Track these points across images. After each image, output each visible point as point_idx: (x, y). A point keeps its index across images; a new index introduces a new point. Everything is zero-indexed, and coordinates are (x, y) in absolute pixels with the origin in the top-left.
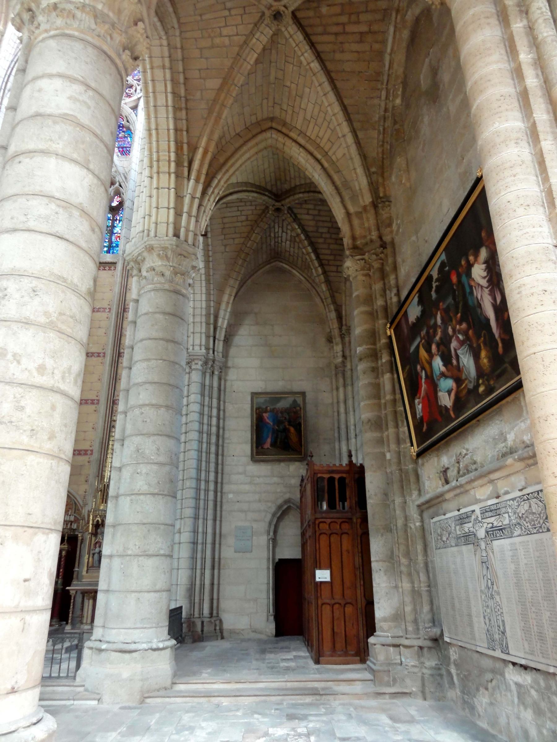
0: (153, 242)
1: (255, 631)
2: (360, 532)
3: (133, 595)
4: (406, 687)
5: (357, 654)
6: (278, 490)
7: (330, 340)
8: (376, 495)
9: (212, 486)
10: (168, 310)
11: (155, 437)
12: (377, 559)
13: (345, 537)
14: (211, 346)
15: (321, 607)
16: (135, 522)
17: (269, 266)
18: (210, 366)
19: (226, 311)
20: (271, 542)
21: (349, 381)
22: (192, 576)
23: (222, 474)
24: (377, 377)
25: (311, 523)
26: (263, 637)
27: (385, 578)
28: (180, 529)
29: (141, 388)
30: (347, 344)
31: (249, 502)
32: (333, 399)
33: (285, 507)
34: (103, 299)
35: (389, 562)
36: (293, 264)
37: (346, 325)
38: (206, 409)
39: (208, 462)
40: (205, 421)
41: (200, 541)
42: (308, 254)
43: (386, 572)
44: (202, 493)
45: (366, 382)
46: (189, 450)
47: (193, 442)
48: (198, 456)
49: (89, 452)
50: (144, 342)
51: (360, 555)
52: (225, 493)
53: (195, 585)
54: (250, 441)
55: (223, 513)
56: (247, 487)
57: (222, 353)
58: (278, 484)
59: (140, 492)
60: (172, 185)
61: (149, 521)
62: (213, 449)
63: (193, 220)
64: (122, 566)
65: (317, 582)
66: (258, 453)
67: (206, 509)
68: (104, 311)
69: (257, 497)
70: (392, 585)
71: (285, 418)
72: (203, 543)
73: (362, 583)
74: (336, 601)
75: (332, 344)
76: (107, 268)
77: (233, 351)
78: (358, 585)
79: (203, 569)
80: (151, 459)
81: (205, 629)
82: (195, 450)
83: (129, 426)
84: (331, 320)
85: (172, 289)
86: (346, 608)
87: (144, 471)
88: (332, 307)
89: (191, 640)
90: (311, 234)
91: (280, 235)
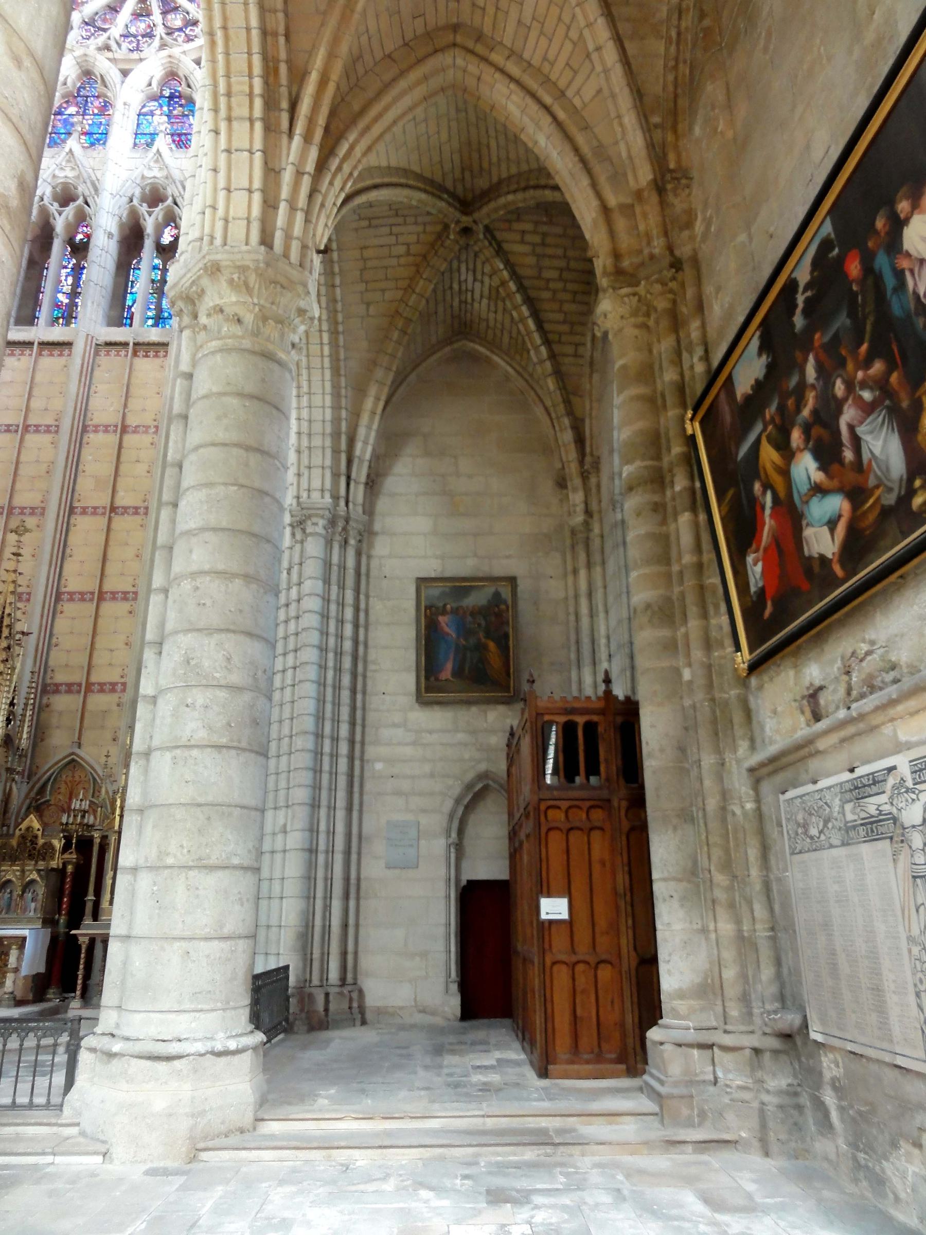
0: (219, 257)
1: (423, 1011)
2: (626, 825)
3: (177, 944)
4: (728, 1129)
5: (621, 1060)
6: (467, 756)
7: (562, 483)
8: (662, 750)
9: (344, 748)
10: (250, 388)
11: (223, 636)
12: (666, 875)
13: (596, 835)
14: (343, 492)
15: (551, 968)
16: (182, 801)
17: (447, 349)
18: (340, 529)
19: (369, 427)
20: (452, 850)
21: (597, 557)
22: (308, 911)
23: (364, 726)
24: (664, 522)
25: (530, 808)
26: (439, 1021)
27: (681, 913)
28: (285, 826)
29: (194, 540)
30: (594, 490)
31: (413, 777)
32: (566, 590)
33: (480, 786)
34: (144, 410)
35: (689, 881)
36: (494, 345)
37: (592, 455)
38: (333, 607)
39: (337, 704)
40: (332, 629)
41: (322, 846)
42: (523, 320)
43: (683, 899)
44: (326, 760)
45: (643, 532)
46: (300, 681)
47: (308, 668)
48: (319, 693)
49: (119, 687)
50: (201, 450)
51: (626, 868)
52: (368, 761)
53: (313, 926)
54: (414, 665)
55: (365, 797)
56: (408, 751)
57: (363, 505)
58: (466, 745)
59: (193, 742)
60: (258, 144)
61: (210, 799)
62: (346, 680)
63: (300, 217)
64: (155, 888)
65: (543, 922)
66: (428, 690)
67: (333, 789)
68: (146, 432)
69: (427, 768)
70: (695, 927)
71: (479, 625)
73: (630, 922)
74: (581, 957)
75: (565, 491)
76: (152, 354)
77: (382, 504)
78: (623, 928)
79: (327, 898)
80: (214, 678)
81: (332, 1007)
82: (313, 681)
83: (172, 615)
84: (564, 445)
85: (257, 348)
86: (600, 972)
87: (200, 701)
88: (566, 421)
89: (305, 1028)
90: (527, 283)
91: (470, 287)
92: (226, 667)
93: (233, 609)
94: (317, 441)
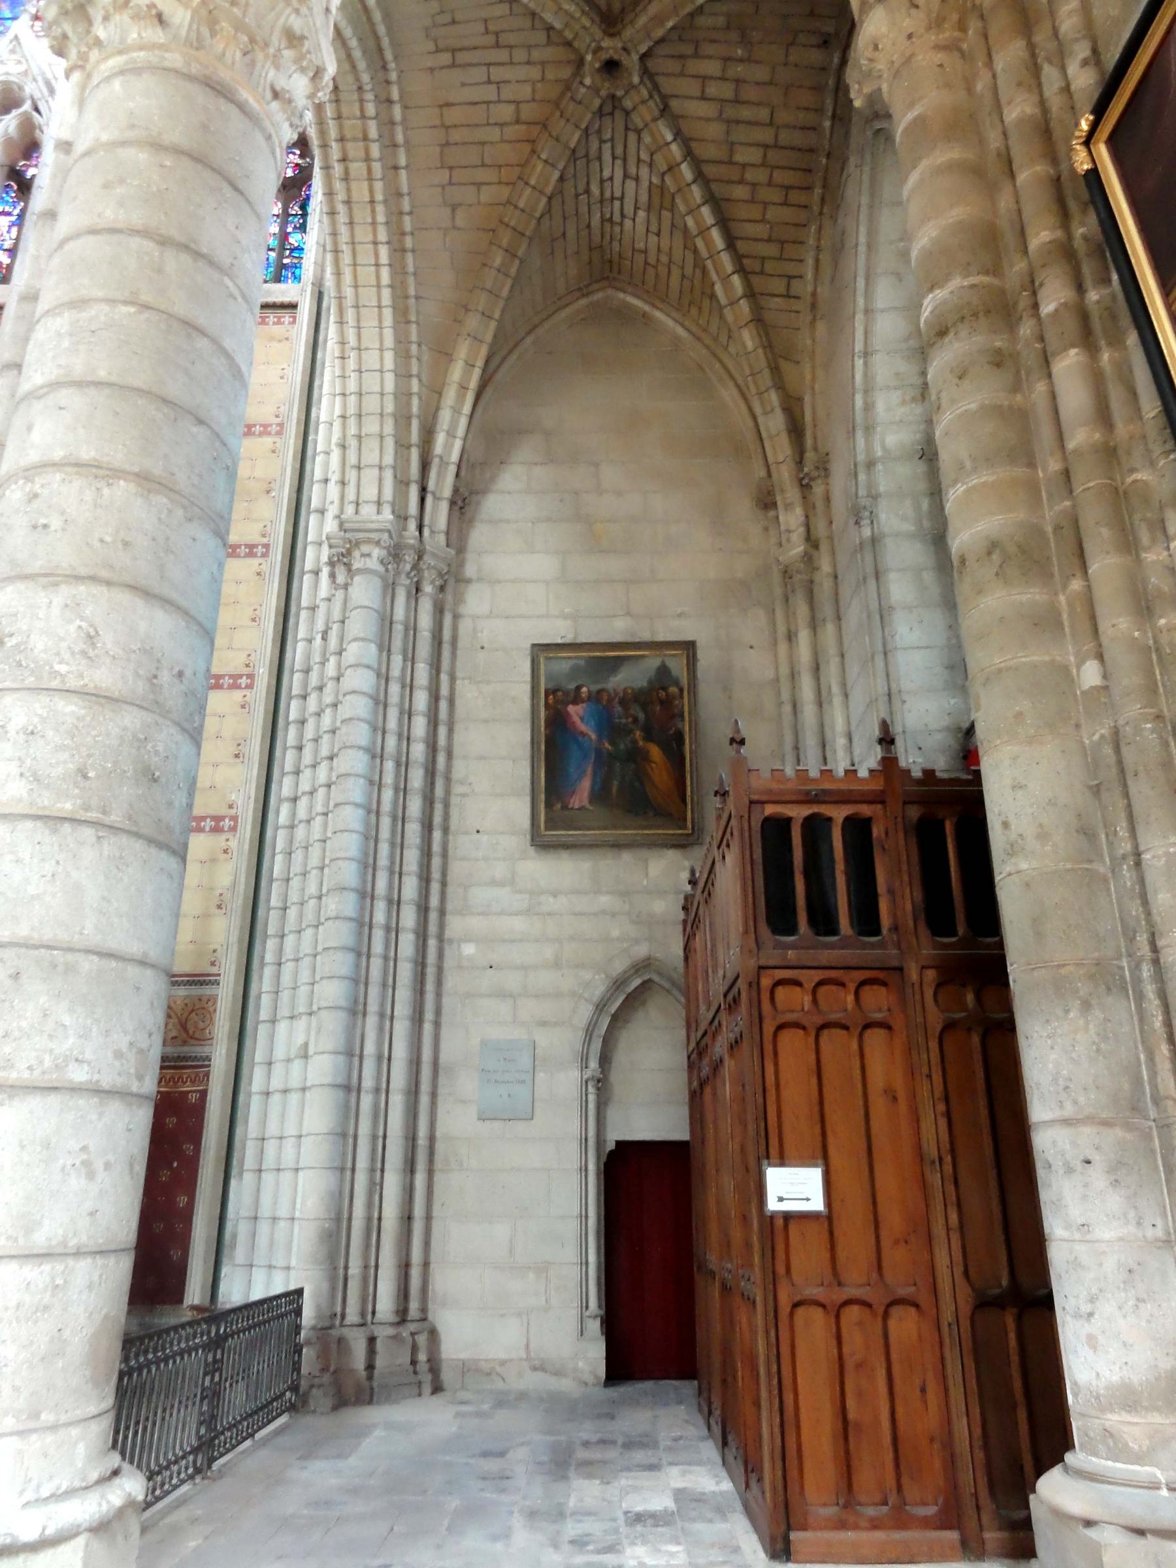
1: (540, 1367)
2: (936, 1019)
5: (949, 1518)
6: (615, 933)
7: (767, 502)
8: (1043, 836)
9: (409, 917)
10: (174, 136)
12: (1069, 1111)
13: (876, 1039)
14: (413, 508)
15: (791, 1314)
17: (583, 302)
18: (408, 567)
19: (456, 411)
20: (591, 1089)
21: (827, 610)
22: (341, 1193)
23: (444, 884)
24: (1016, 388)
25: (741, 984)
26: (566, 1385)
27: (1115, 1201)
28: (306, 1045)
29: (38, 406)
30: (820, 505)
31: (524, 968)
32: (777, 669)
33: (637, 982)
35: (1129, 1127)
36: (657, 294)
37: (816, 449)
38: (394, 689)
39: (398, 844)
40: (392, 724)
41: (368, 1083)
42: (703, 232)
43: (1115, 1168)
44: (378, 935)
45: (973, 406)
46: (336, 805)
47: (351, 782)
48: (367, 824)
51: (941, 1107)
52: (451, 941)
53: (350, 1219)
54: (528, 782)
55: (446, 1001)
56: (518, 924)
57: (447, 533)
58: (613, 915)
61: (23, 931)
62: (415, 806)
65: (773, 1216)
66: (551, 823)
67: (389, 984)
69: (549, 952)
70: (1150, 1233)
71: (636, 720)
72: (377, 1090)
73: (954, 1217)
74: (851, 1292)
75: (772, 513)
77: (479, 535)
78: (939, 1230)
79: (378, 1168)
80: (55, 674)
81: (380, 1362)
82: (357, 805)
84: (771, 437)
85: (195, 69)
86: (892, 1323)
88: (774, 397)
89: (329, 1402)
90: (710, 170)
91: (618, 194)
92: (84, 653)
93: (108, 539)
94: (372, 426)
